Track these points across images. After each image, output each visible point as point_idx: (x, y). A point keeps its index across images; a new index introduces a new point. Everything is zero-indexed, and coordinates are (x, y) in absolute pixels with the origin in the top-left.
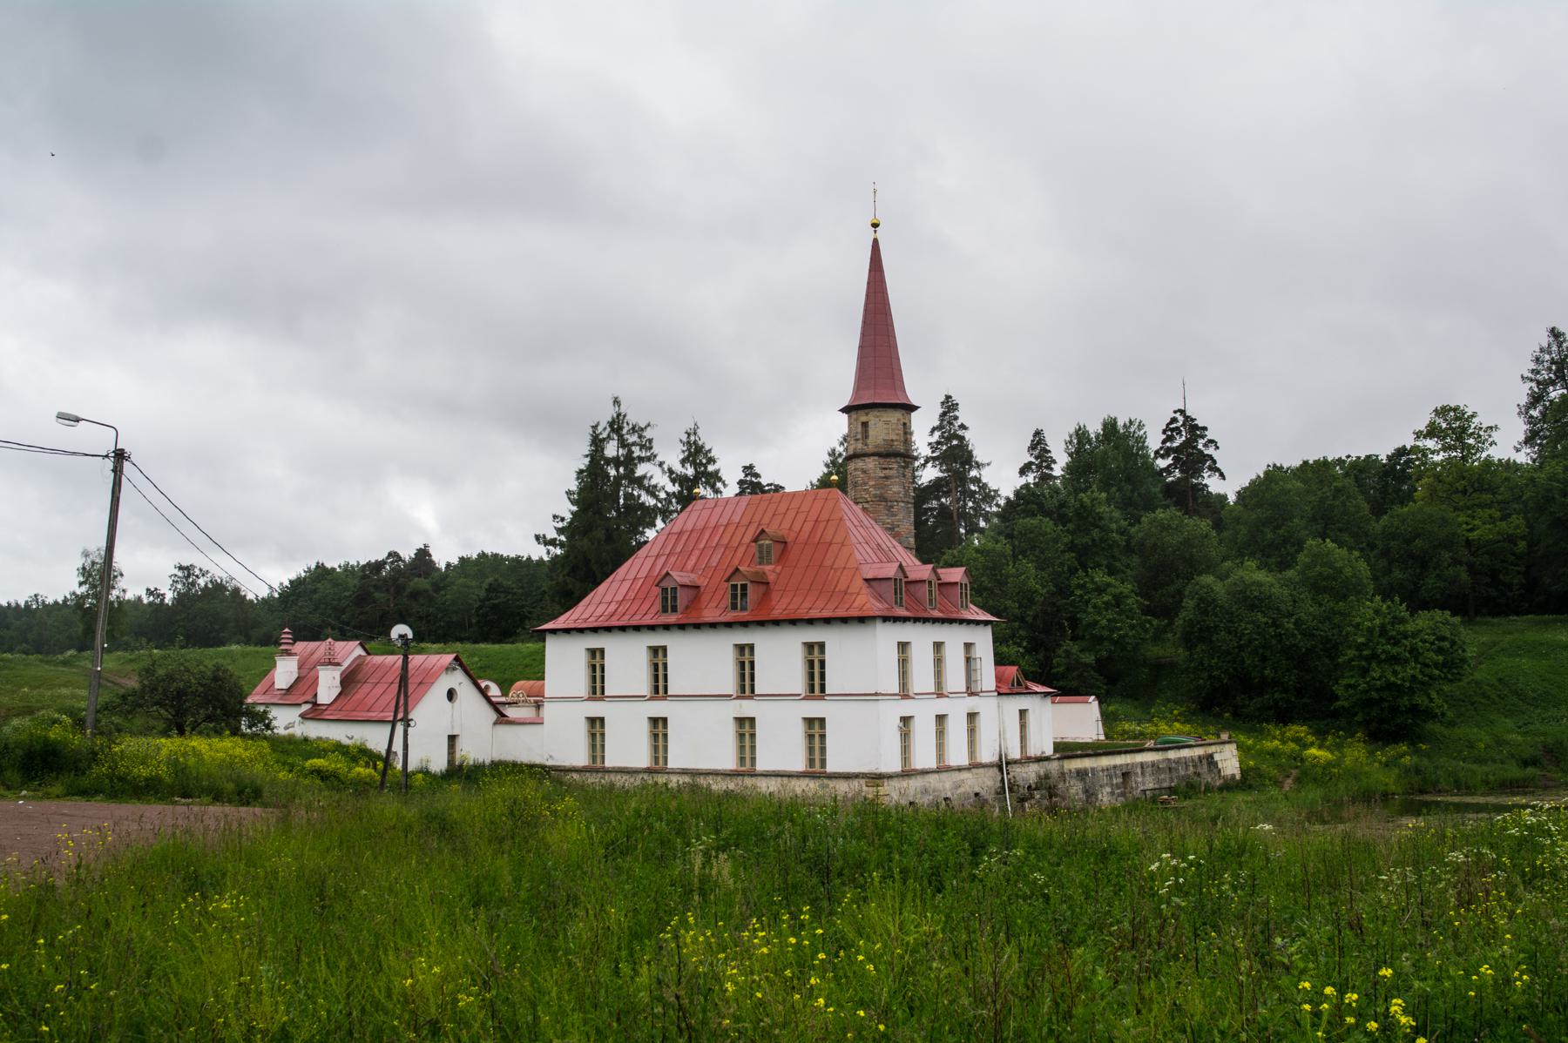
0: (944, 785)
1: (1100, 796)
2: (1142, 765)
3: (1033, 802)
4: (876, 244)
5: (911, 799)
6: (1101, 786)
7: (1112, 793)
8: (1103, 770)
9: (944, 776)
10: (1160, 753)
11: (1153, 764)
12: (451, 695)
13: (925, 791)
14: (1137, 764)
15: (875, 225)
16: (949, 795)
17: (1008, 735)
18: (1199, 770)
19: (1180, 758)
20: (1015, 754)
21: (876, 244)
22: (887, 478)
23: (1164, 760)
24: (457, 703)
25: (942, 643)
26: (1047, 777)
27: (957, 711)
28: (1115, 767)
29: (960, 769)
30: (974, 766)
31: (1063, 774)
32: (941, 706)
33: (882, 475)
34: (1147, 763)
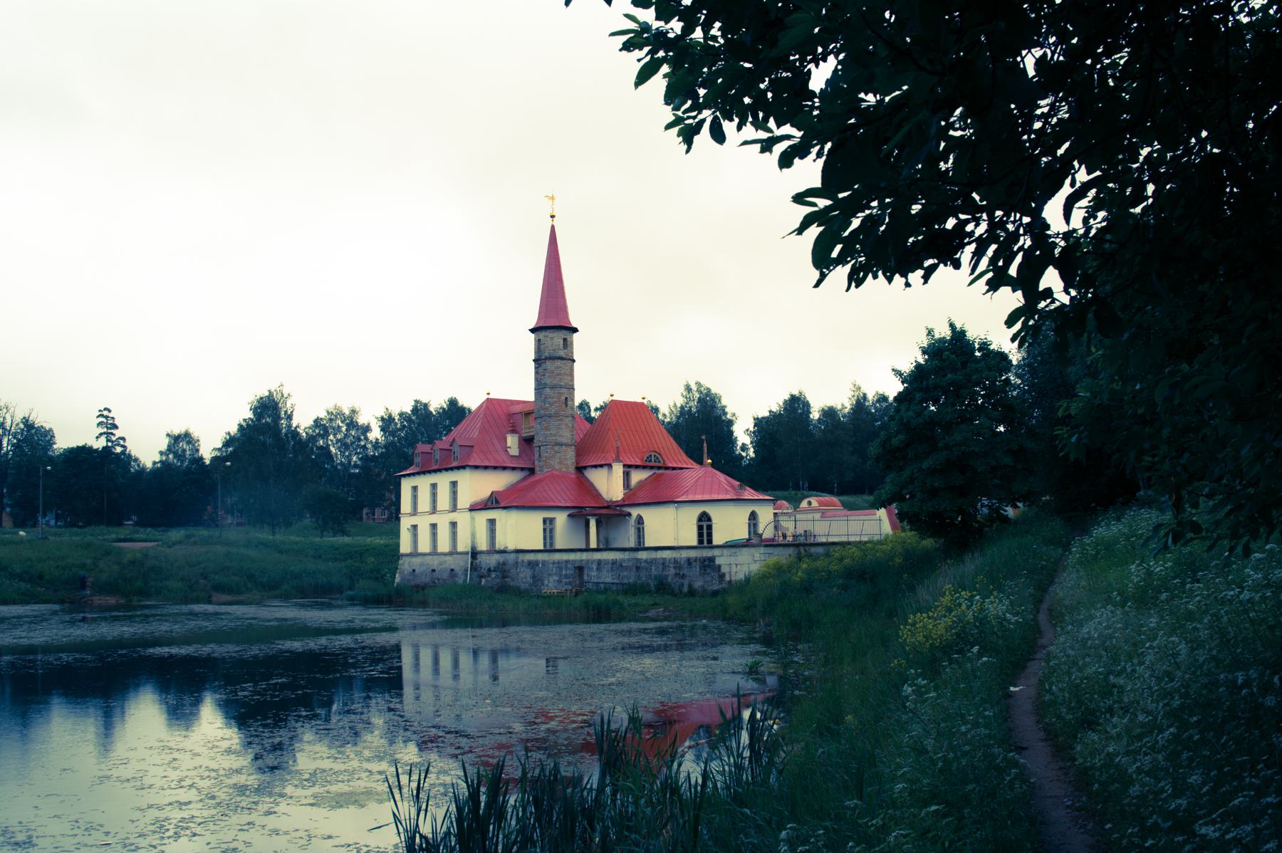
0: (434, 562)
1: (546, 582)
2: (599, 562)
3: (489, 579)
6: (549, 575)
7: (560, 581)
8: (554, 563)
9: (435, 557)
10: (627, 553)
11: (614, 562)
13: (422, 565)
14: (594, 561)
16: (435, 568)
17: (478, 536)
18: (685, 571)
19: (656, 559)
20: (483, 545)
23: (629, 560)
25: (457, 482)
26: (504, 564)
27: (443, 522)
28: (567, 562)
29: (445, 554)
30: (453, 552)
31: (517, 563)
32: (434, 519)
34: (605, 560)
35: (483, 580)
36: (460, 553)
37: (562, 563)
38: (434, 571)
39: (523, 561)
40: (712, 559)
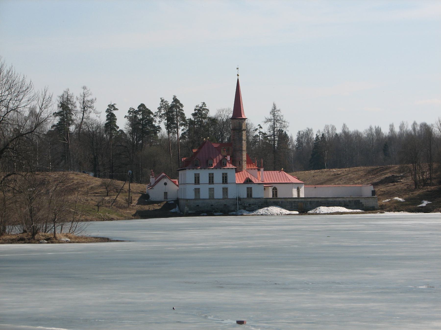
2: (310, 202)
4: (238, 80)
5: (198, 205)
8: (287, 202)
12: (165, 184)
14: (307, 202)
15: (238, 75)
19: (336, 201)
21: (238, 80)
22: (234, 135)
24: (167, 186)
29: (219, 199)
33: (233, 134)
35: (247, 208)
36: (230, 199)
37: (292, 202)
38: (212, 205)
39: (270, 202)
40: (359, 201)
